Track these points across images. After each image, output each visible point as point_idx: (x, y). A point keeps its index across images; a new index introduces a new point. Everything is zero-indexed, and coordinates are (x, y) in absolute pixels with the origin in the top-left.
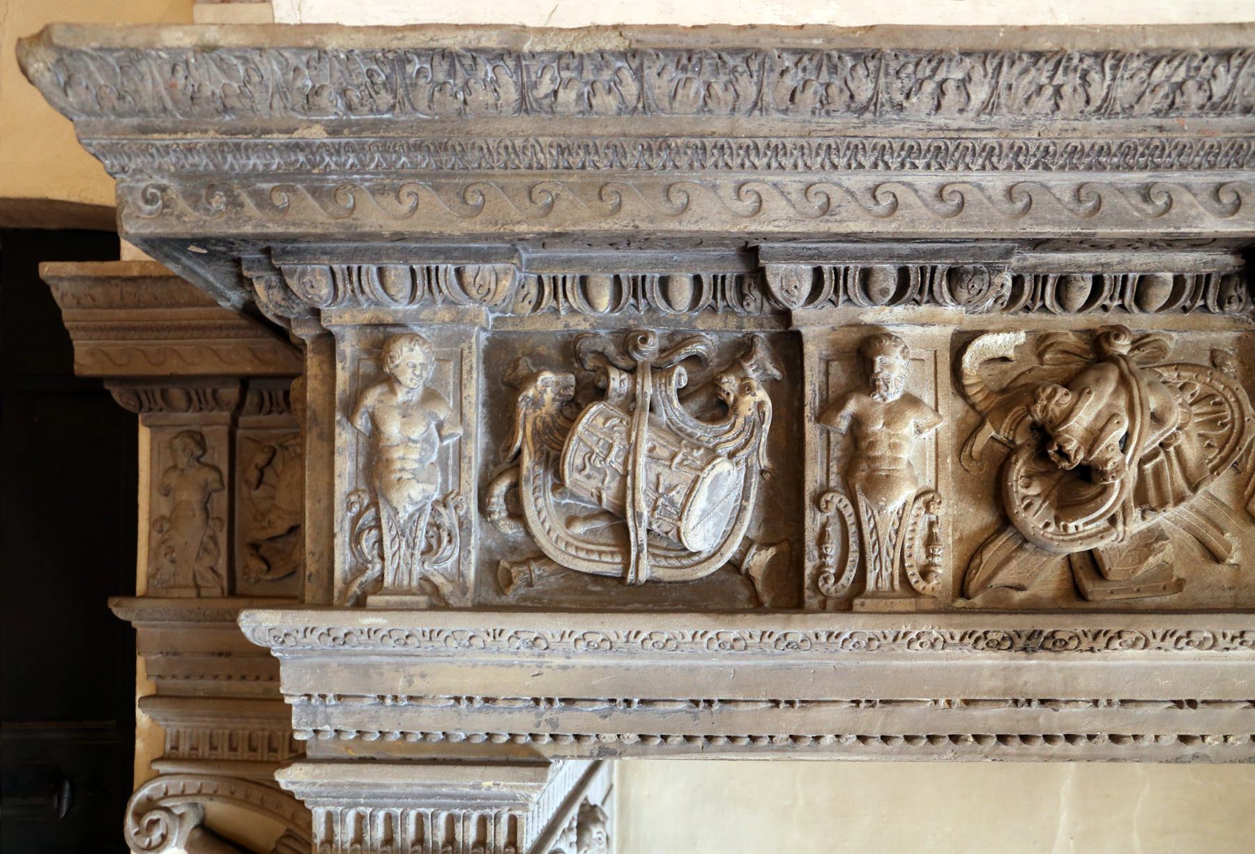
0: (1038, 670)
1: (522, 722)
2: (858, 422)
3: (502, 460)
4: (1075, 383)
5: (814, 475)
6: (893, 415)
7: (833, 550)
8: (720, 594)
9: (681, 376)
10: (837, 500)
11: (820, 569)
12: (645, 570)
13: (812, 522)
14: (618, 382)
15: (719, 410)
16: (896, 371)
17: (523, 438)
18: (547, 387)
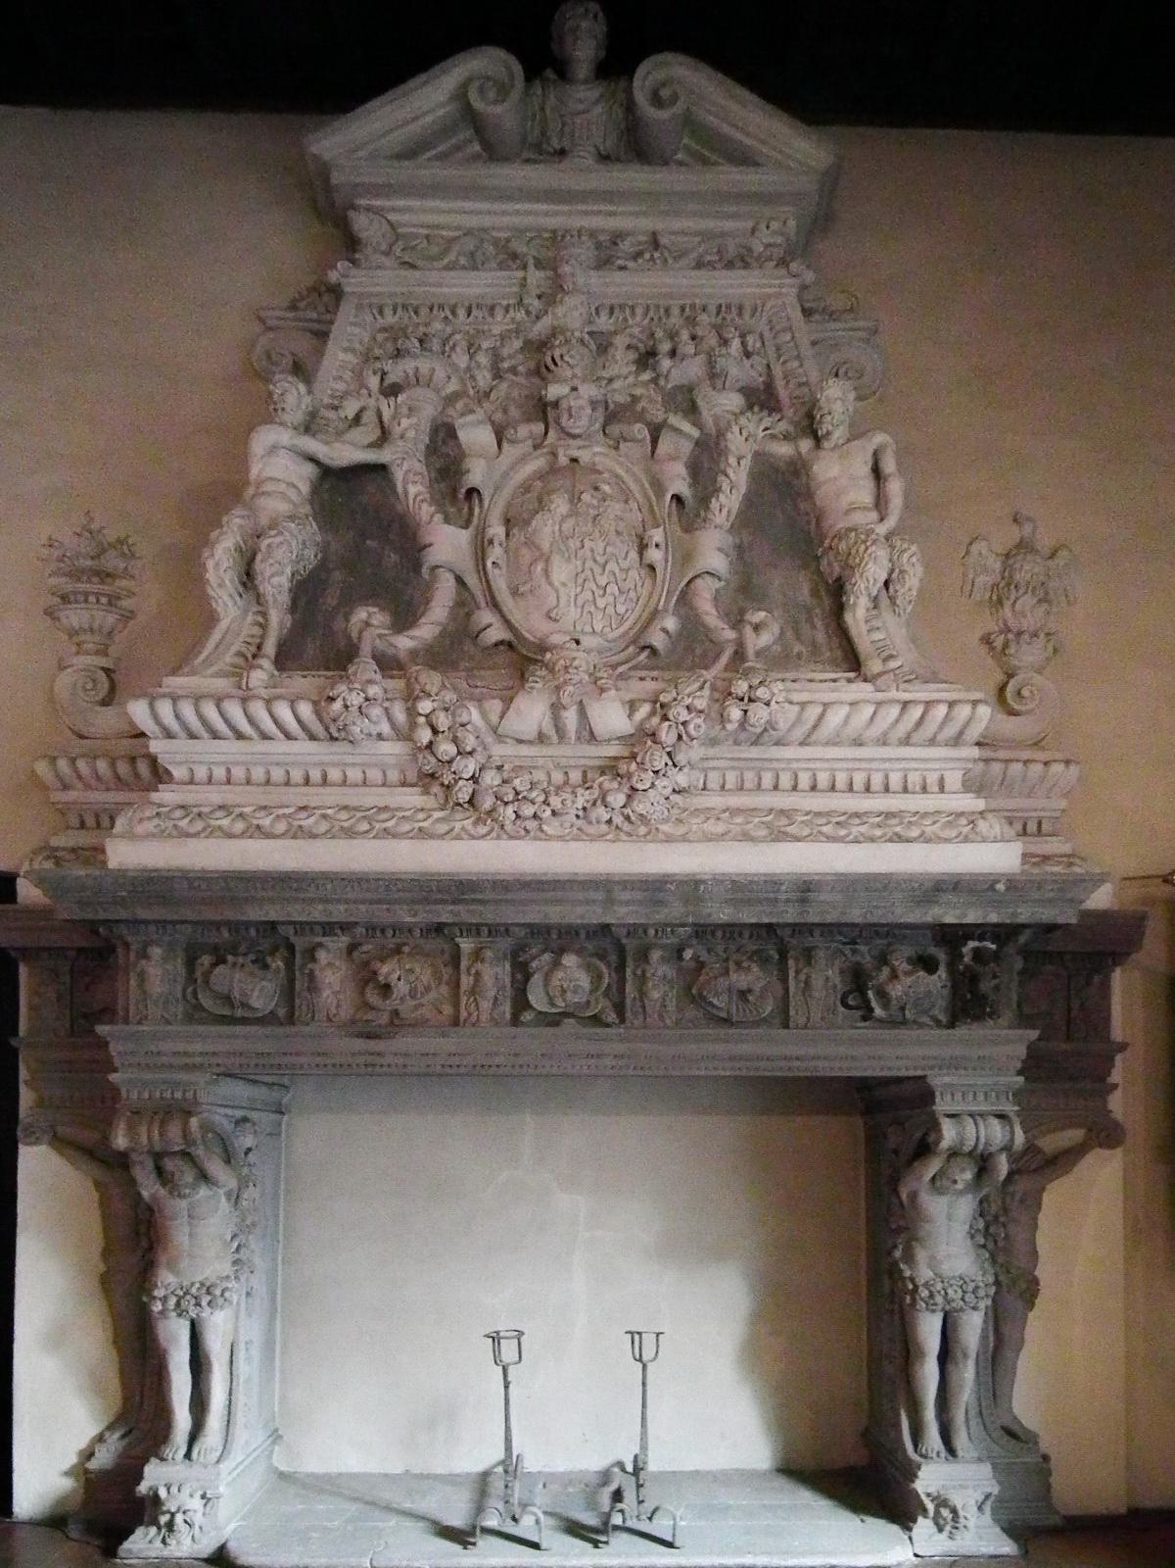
0: (373, 1045)
1: (198, 1060)
2: (312, 971)
3: (191, 979)
4: (383, 960)
5: (298, 986)
6: (322, 970)
7: (304, 1008)
8: (268, 1019)
9: (251, 957)
10: (305, 994)
11: (300, 1015)
12: (239, 1013)
13: (297, 1001)
14: (230, 958)
15: (266, 967)
16: (322, 956)
17: (198, 974)
18: (206, 960)
